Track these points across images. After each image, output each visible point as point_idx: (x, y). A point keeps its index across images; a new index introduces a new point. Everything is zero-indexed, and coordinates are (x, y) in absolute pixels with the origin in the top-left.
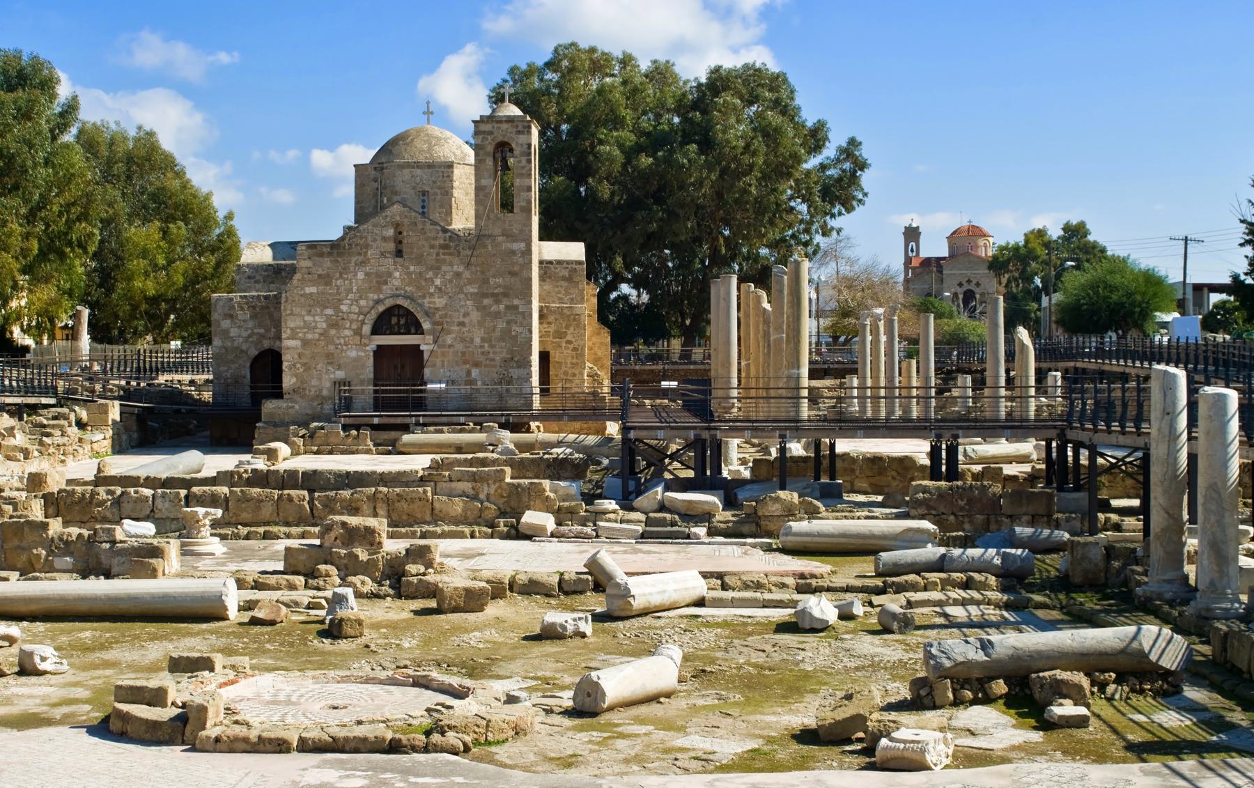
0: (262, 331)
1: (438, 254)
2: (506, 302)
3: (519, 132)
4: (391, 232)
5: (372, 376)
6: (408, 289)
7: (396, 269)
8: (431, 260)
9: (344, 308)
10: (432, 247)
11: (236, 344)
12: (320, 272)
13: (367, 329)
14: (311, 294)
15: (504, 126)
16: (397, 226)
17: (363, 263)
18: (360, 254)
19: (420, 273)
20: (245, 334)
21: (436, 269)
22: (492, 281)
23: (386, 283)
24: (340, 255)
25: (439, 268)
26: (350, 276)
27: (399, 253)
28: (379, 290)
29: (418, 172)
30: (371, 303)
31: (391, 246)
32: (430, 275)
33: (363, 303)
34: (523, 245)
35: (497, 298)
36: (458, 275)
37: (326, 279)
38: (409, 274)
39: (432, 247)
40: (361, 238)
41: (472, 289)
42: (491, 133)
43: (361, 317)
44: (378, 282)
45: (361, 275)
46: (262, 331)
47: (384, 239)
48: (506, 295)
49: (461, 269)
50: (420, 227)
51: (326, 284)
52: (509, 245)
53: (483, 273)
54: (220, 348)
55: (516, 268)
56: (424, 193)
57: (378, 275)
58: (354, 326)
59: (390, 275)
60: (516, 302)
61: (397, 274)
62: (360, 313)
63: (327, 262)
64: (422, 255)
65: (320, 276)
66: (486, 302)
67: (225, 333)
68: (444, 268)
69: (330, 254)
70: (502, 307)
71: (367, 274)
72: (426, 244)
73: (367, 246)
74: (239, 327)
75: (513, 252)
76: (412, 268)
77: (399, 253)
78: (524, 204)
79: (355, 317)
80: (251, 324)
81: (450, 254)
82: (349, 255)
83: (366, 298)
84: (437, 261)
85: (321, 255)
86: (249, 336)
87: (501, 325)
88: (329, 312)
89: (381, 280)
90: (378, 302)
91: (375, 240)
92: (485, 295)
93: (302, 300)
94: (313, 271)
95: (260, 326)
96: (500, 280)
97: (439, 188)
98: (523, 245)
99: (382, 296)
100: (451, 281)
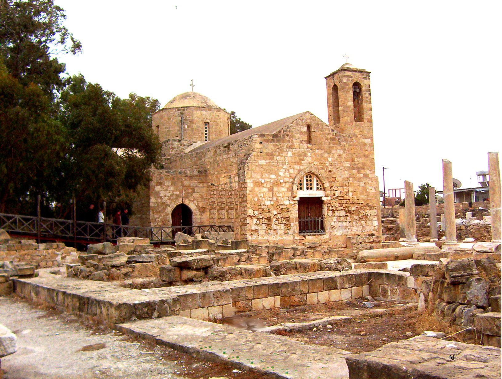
0: (178, 193)
1: (329, 144)
2: (362, 171)
3: (364, 78)
4: (305, 129)
5: (297, 216)
6: (316, 163)
7: (309, 151)
8: (326, 147)
9: (281, 174)
10: (327, 139)
11: (163, 201)
12: (267, 151)
13: (295, 187)
14: (263, 165)
15: (357, 74)
16: (309, 127)
17: (291, 147)
18: (289, 141)
19: (321, 155)
20: (169, 195)
21: (329, 152)
22: (356, 160)
23: (303, 160)
24: (278, 141)
25: (330, 152)
26: (284, 154)
27: (309, 141)
28: (300, 164)
29: (204, 113)
30: (296, 172)
31: (305, 137)
32: (326, 155)
33: (291, 171)
34: (369, 140)
35: (359, 170)
36: (340, 156)
37: (270, 156)
38: (316, 154)
39: (327, 139)
40: (289, 131)
41: (347, 164)
42: (351, 77)
43: (291, 180)
44: (300, 159)
45: (290, 154)
46: (178, 193)
47: (302, 133)
48: (363, 168)
49: (341, 152)
50: (320, 127)
51: (271, 159)
52: (363, 140)
53: (352, 155)
54: (154, 203)
55: (367, 153)
56: (206, 123)
57: (299, 155)
58: (287, 186)
59: (305, 155)
60: (368, 172)
61: (309, 154)
62: (291, 177)
63: (270, 147)
64: (321, 144)
65: (267, 154)
66: (354, 172)
67: (158, 193)
68: (333, 152)
69: (272, 140)
70: (361, 175)
71: (293, 154)
72: (323, 136)
73: (293, 137)
74: (166, 190)
75: (365, 144)
76: (317, 151)
77: (309, 141)
78: (369, 117)
79: (287, 180)
80: (172, 189)
81: (336, 144)
82: (283, 142)
83: (293, 169)
84: (330, 147)
85: (268, 141)
86: (171, 196)
87: (362, 185)
88: (273, 176)
89: (301, 158)
90: (300, 171)
91: (297, 133)
92: (353, 168)
93: (257, 168)
94: (263, 150)
95: (177, 190)
96: (360, 160)
97: (215, 122)
98: (369, 140)
99: (302, 168)
100: (337, 159)
